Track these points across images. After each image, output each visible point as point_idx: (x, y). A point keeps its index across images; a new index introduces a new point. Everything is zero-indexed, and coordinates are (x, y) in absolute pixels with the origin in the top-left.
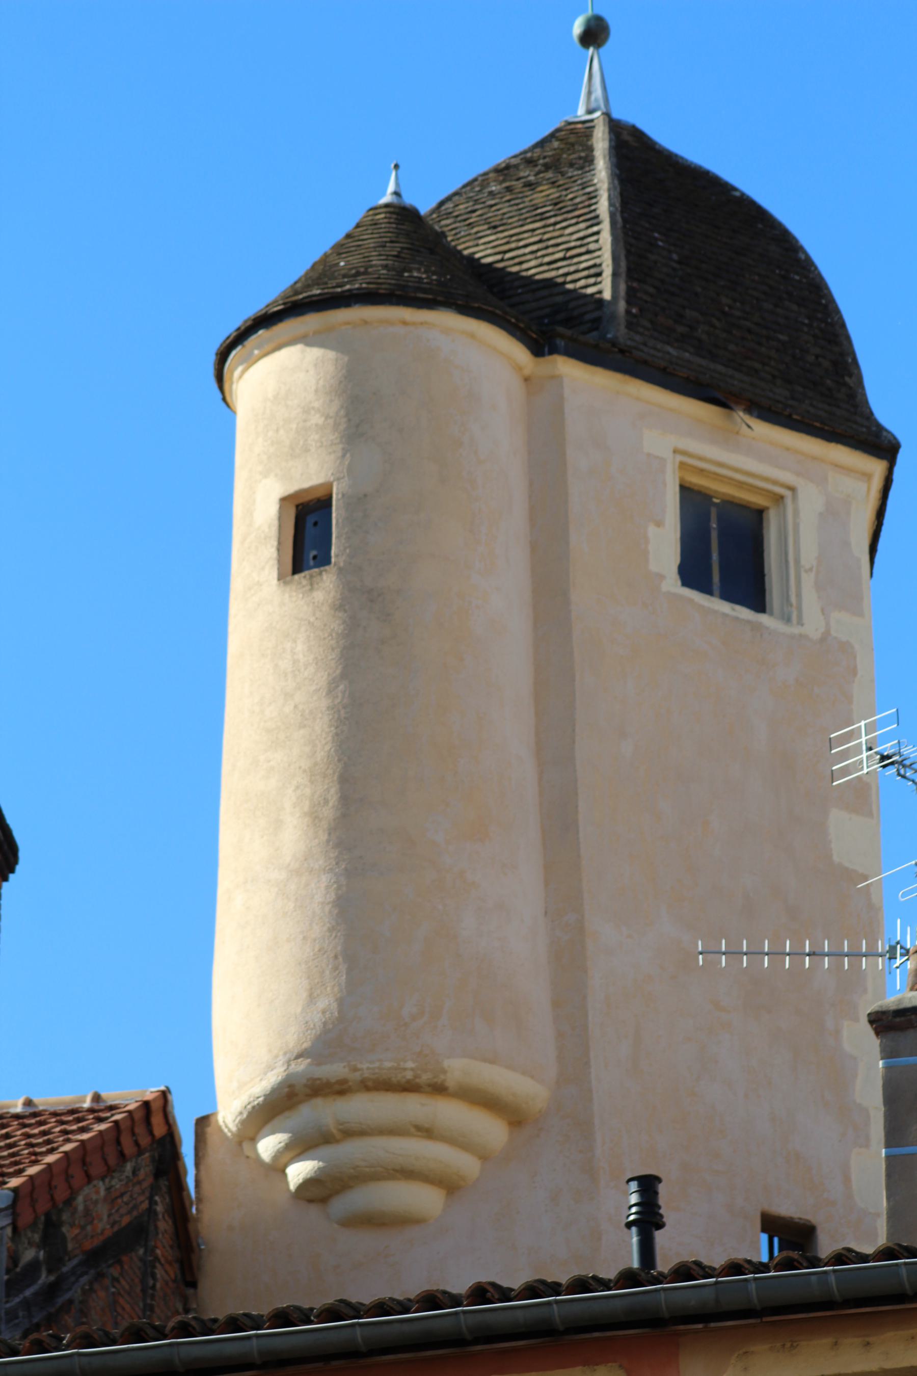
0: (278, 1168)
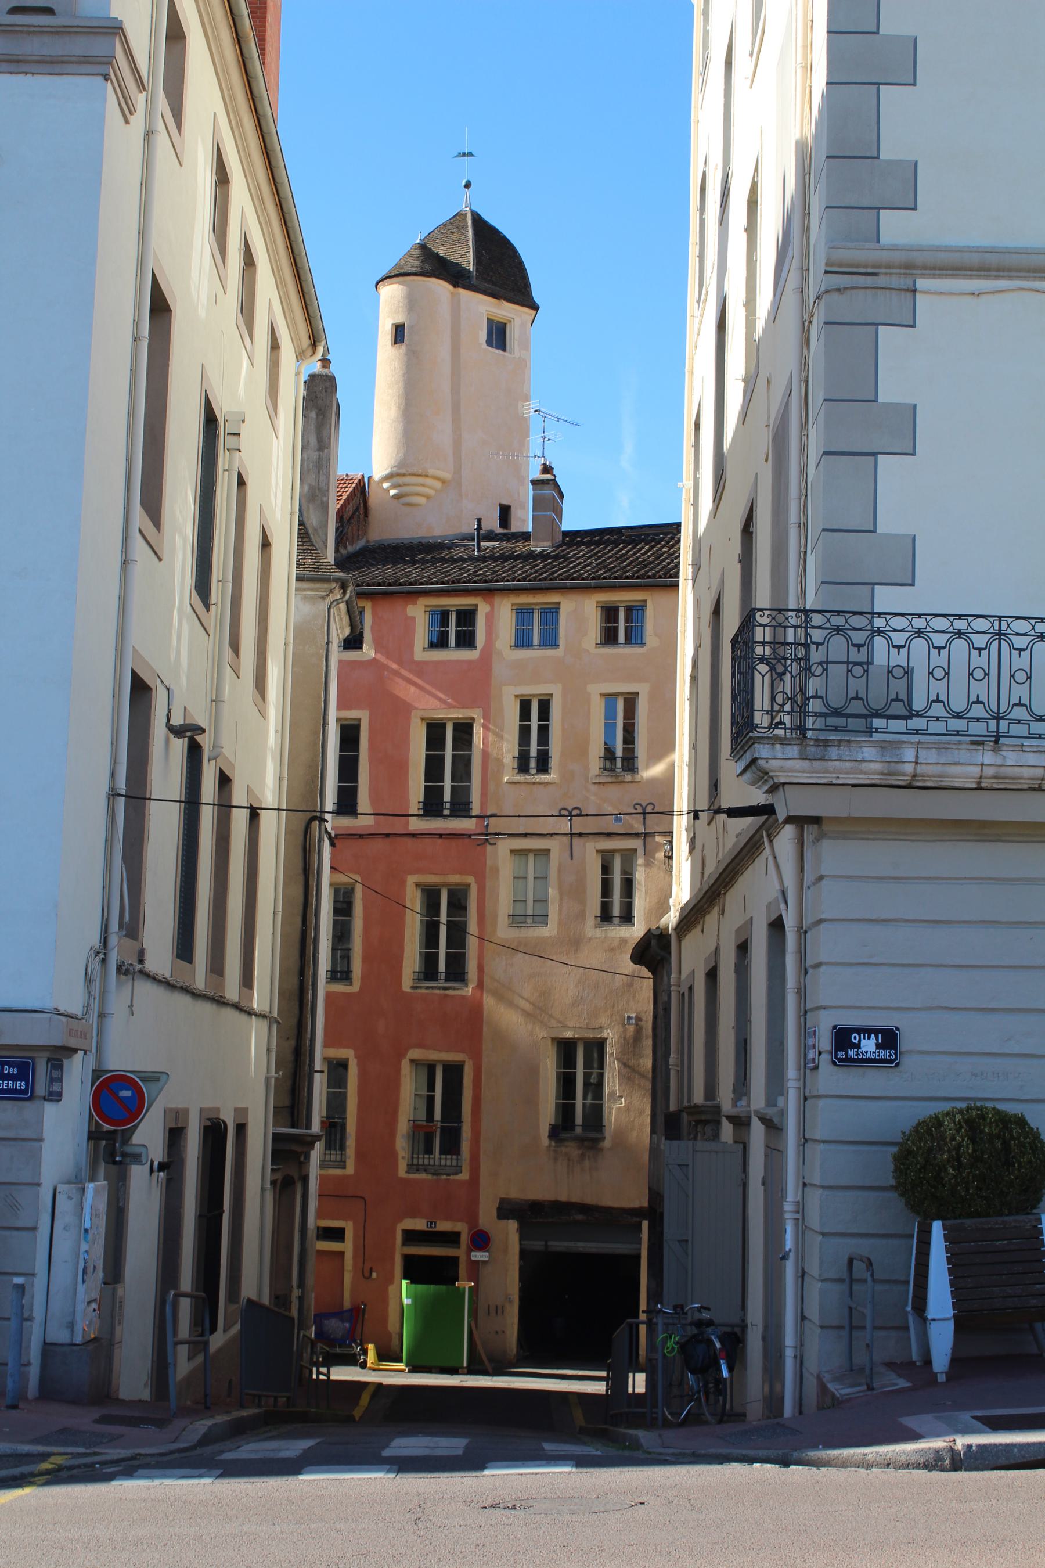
0: (388, 490)
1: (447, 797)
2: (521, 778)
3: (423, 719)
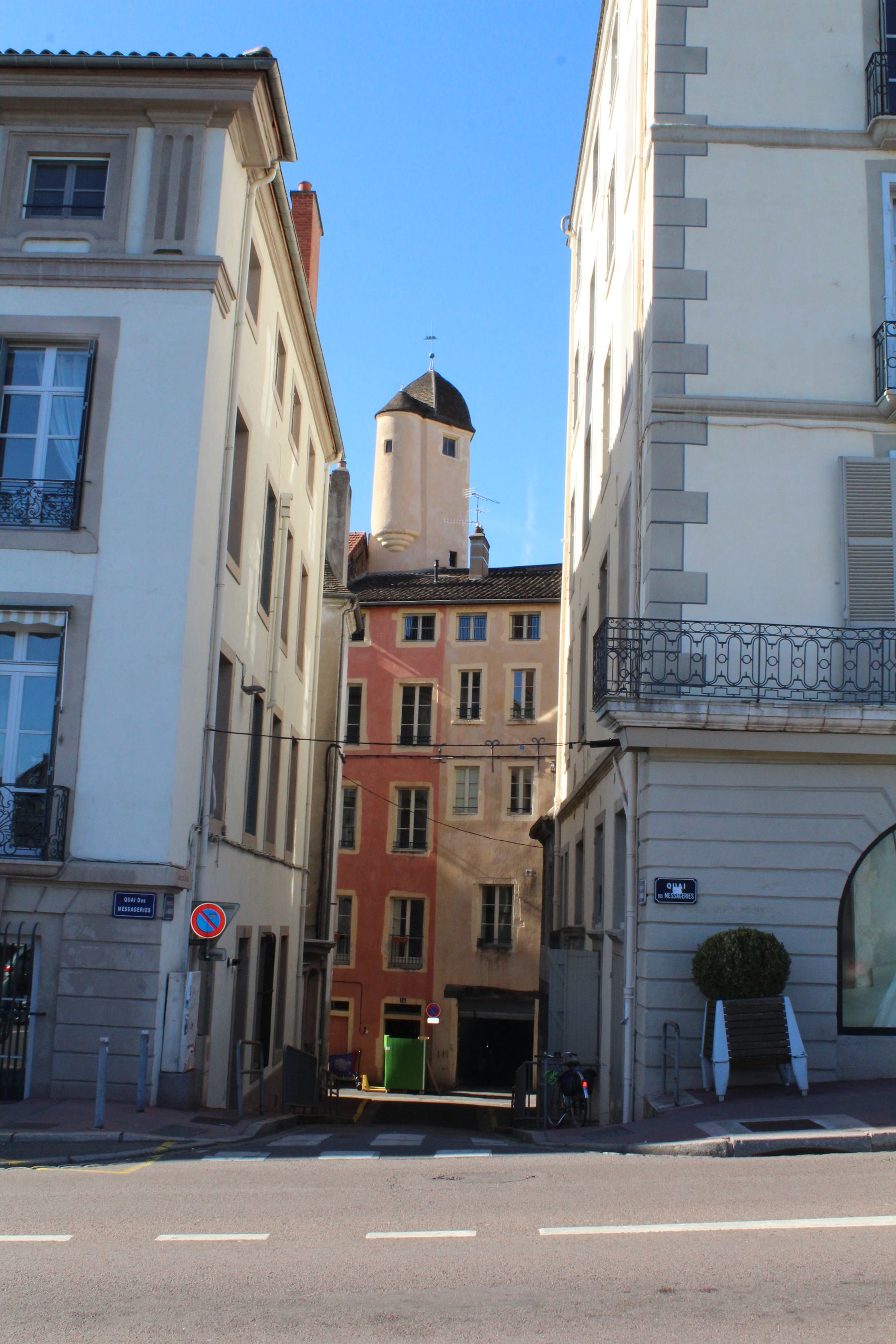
0: (380, 542)
1: (415, 733)
2: (462, 721)
3: (401, 684)
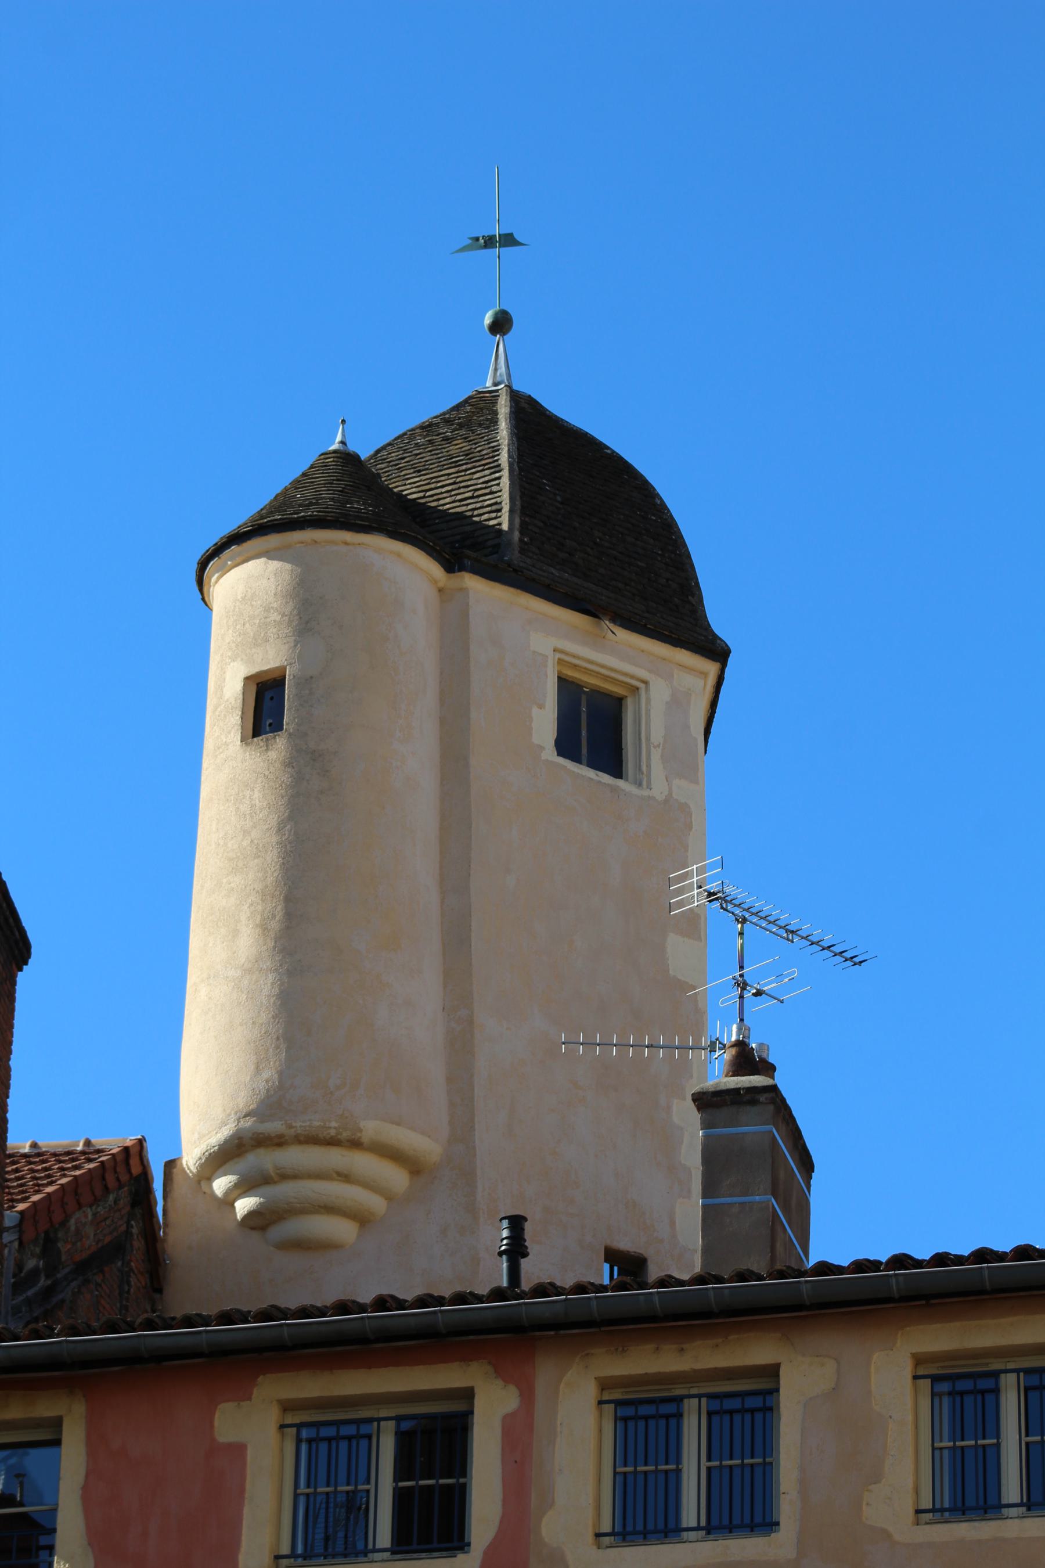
0: (227, 1202)
